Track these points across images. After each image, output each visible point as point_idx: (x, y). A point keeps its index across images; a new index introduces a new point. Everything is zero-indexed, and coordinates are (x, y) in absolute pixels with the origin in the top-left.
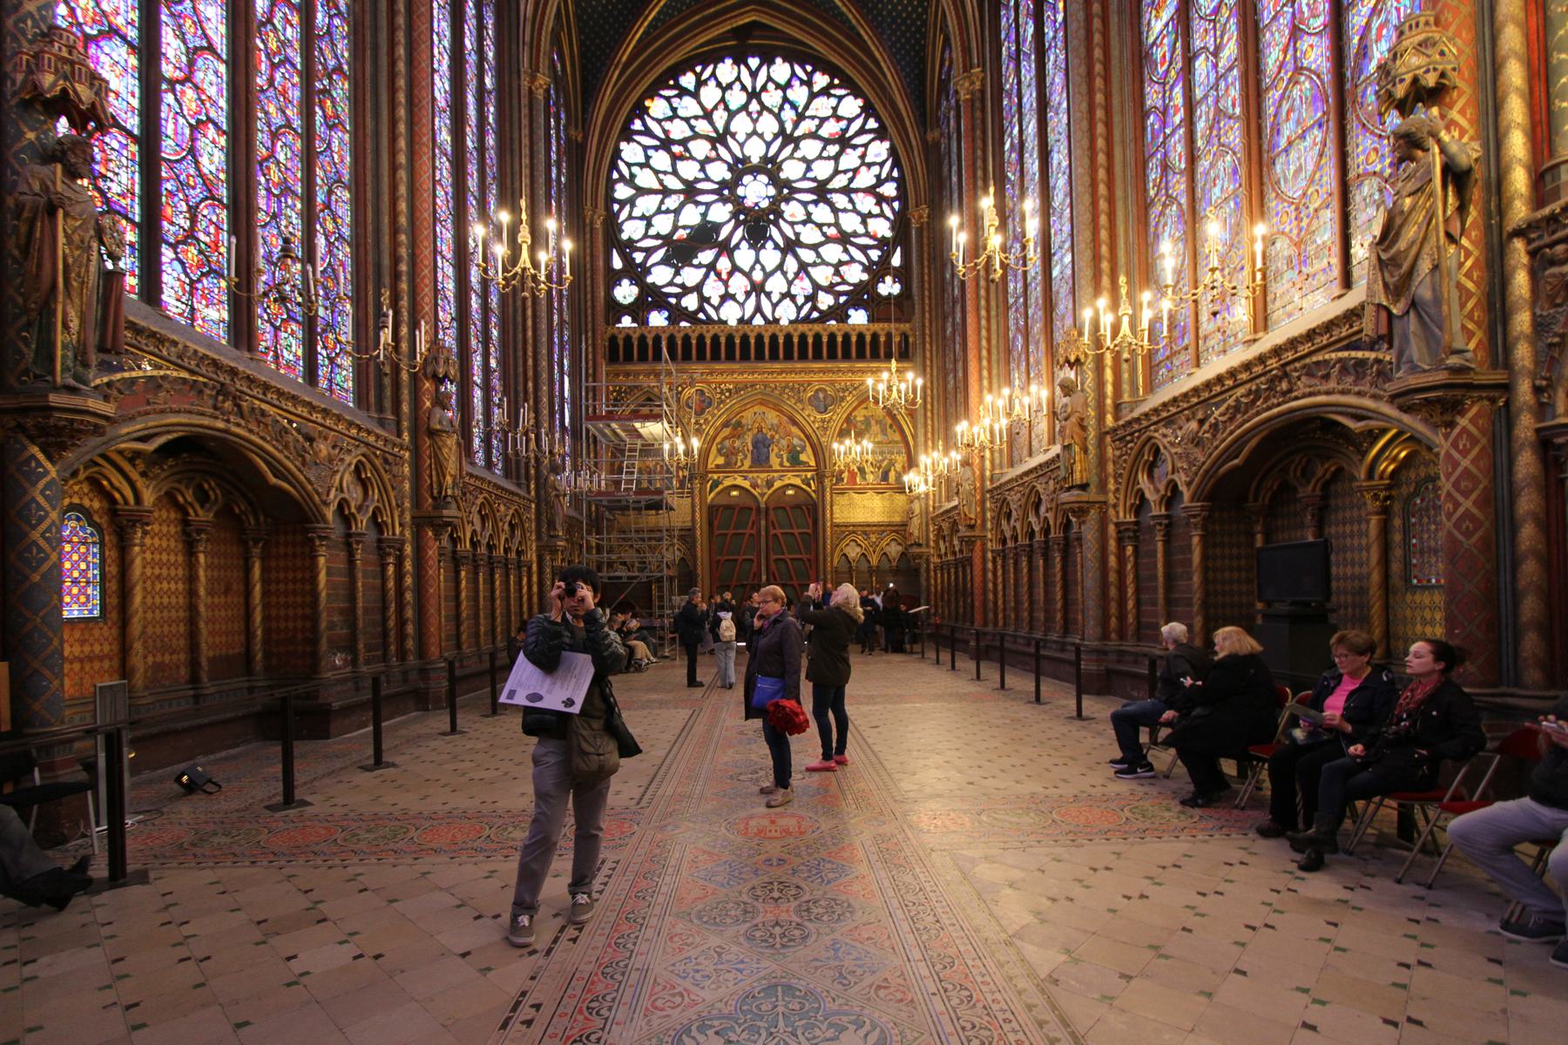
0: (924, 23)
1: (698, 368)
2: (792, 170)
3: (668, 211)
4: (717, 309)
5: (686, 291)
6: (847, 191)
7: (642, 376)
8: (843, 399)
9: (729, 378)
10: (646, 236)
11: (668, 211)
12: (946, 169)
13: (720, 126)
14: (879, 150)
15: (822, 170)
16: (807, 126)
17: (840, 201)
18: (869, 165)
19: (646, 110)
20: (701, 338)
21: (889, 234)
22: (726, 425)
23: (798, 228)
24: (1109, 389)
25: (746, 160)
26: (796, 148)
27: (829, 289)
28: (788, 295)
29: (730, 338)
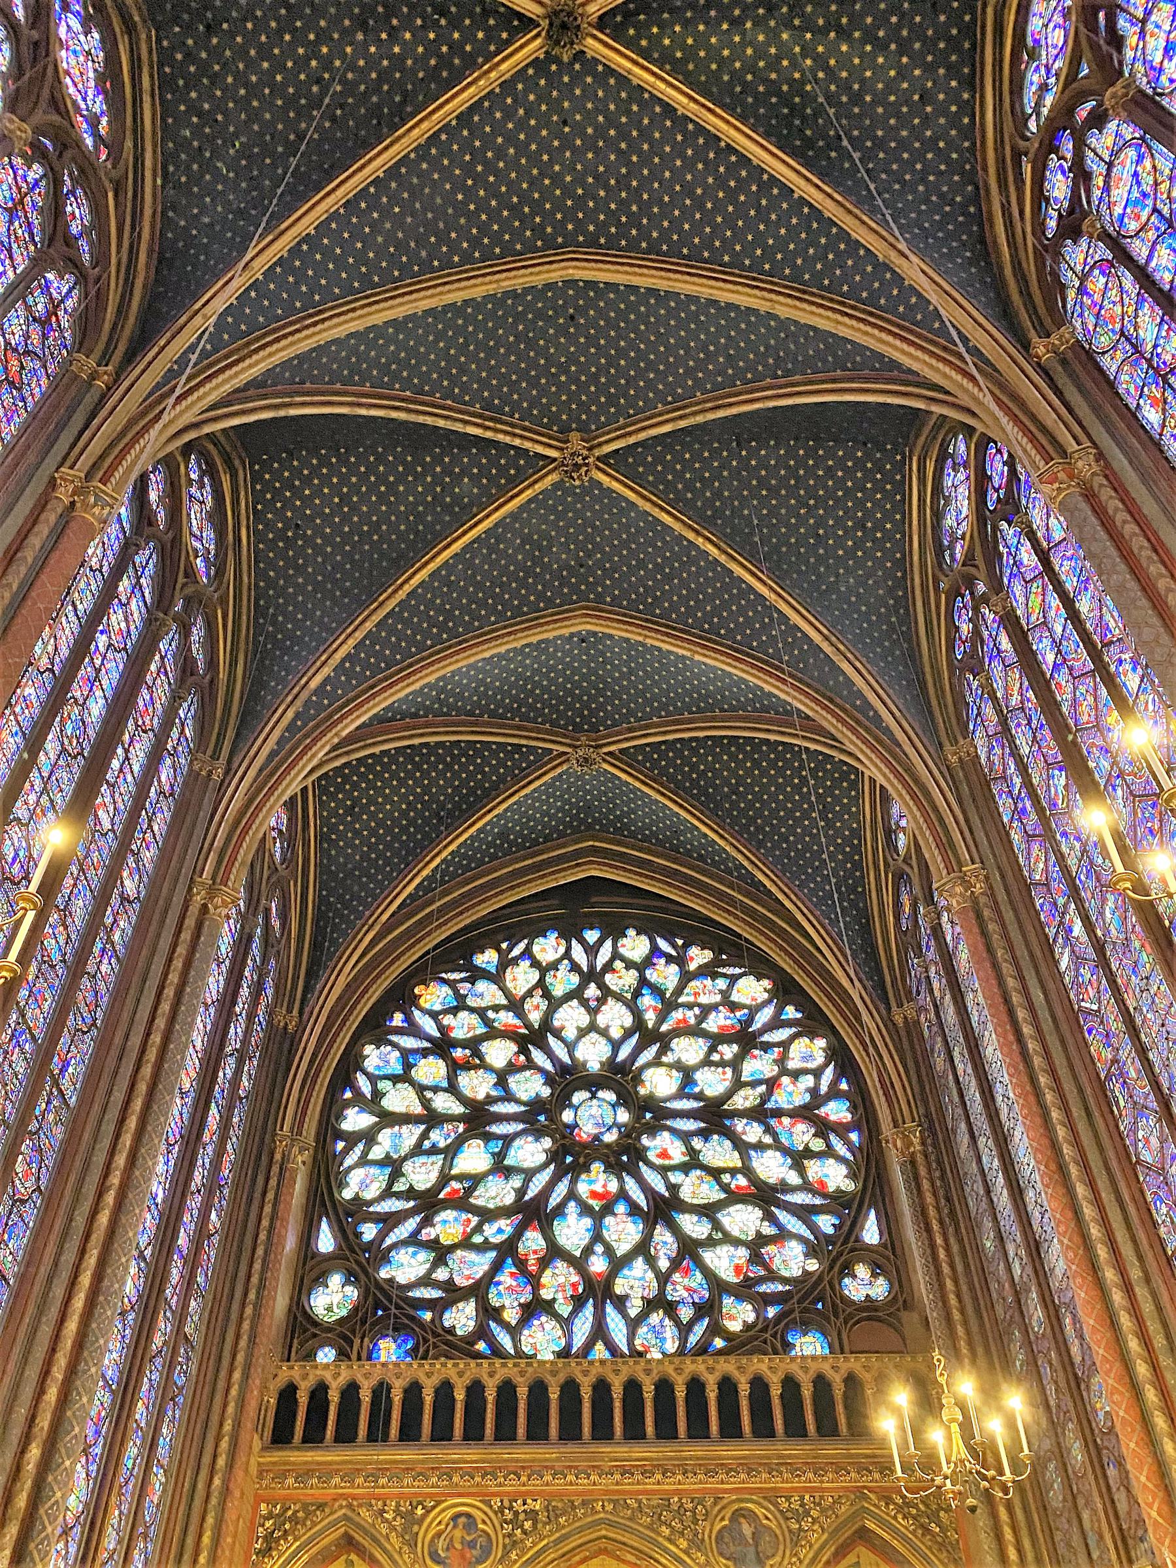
0: (858, 866)
2: (659, 1083)
3: (434, 1150)
4: (514, 1332)
5: (453, 1293)
10: (387, 1193)
11: (434, 1150)
12: (940, 1062)
14: (810, 1051)
15: (712, 1083)
17: (753, 1132)
18: (796, 1075)
19: (414, 1000)
21: (849, 1186)
23: (675, 1178)
26: (665, 1048)
27: (745, 1290)
28: (659, 1303)
29: (538, 1389)
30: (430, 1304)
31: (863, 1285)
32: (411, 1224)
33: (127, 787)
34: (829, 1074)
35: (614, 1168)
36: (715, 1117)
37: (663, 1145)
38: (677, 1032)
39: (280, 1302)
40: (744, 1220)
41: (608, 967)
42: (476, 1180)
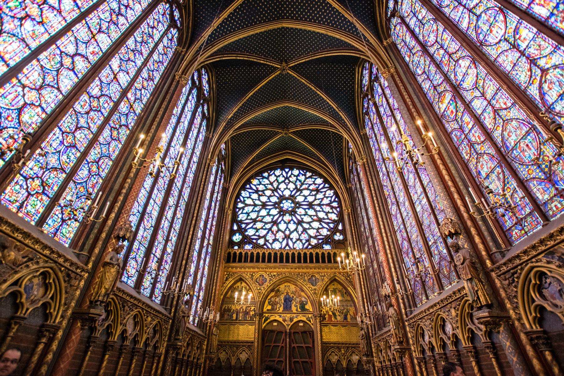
1: (261, 265)
4: (271, 244)
5: (260, 238)
6: (319, 205)
7: (239, 269)
8: (323, 280)
9: (275, 270)
10: (247, 219)
12: (355, 195)
13: (275, 186)
15: (311, 199)
16: (304, 187)
17: (318, 208)
18: (327, 197)
19: (251, 183)
20: (264, 253)
21: (336, 219)
22: (272, 290)
23: (303, 217)
24: (481, 246)
25: (284, 196)
26: (301, 192)
27: (315, 237)
29: (276, 254)
30: (255, 239)
31: (338, 237)
32: (252, 225)
33: (193, 139)
34: (334, 197)
35: (291, 215)
36: (311, 205)
37: (300, 211)
38: (304, 189)
39: (227, 238)
40: (316, 225)
41: (290, 176)
42: (264, 217)
